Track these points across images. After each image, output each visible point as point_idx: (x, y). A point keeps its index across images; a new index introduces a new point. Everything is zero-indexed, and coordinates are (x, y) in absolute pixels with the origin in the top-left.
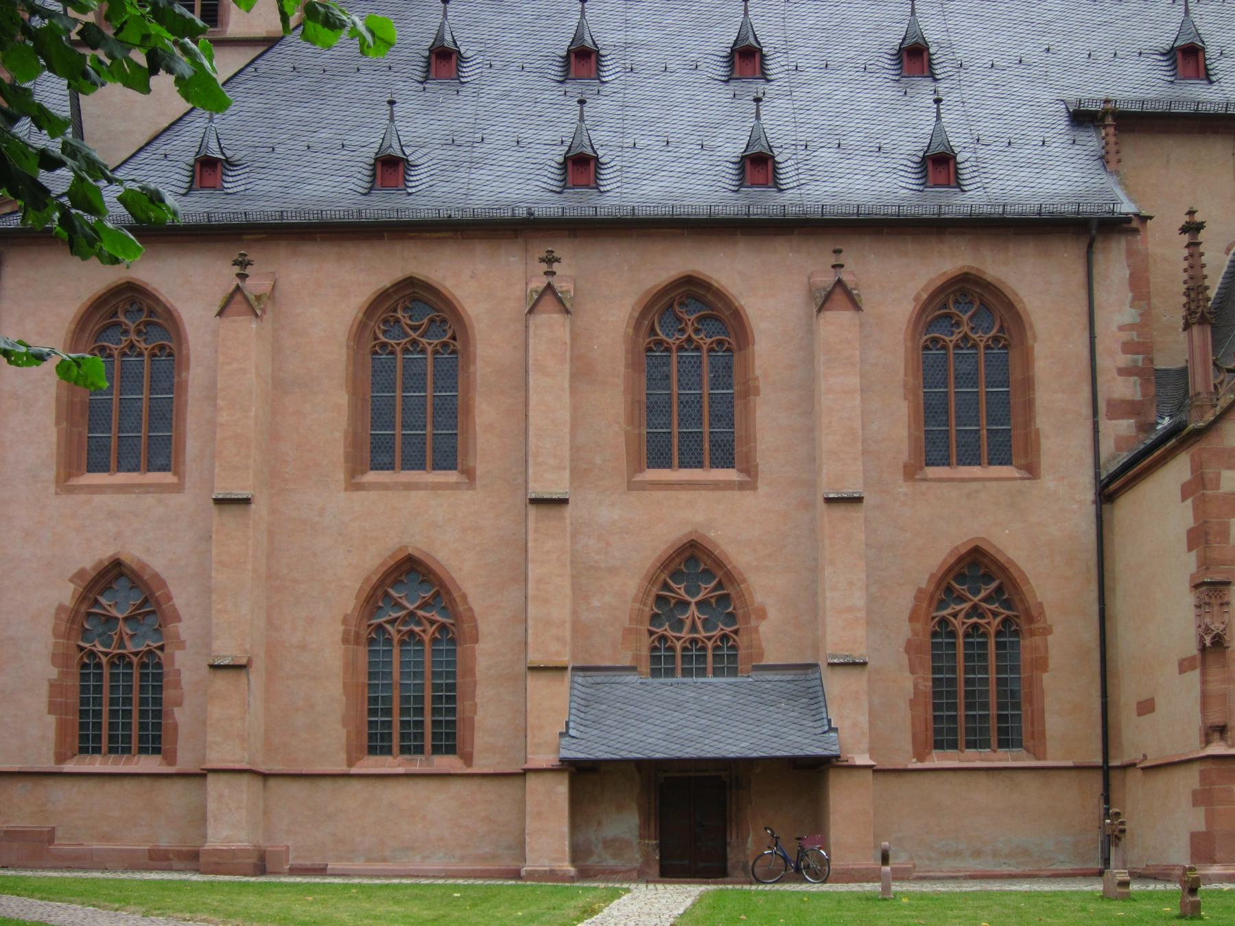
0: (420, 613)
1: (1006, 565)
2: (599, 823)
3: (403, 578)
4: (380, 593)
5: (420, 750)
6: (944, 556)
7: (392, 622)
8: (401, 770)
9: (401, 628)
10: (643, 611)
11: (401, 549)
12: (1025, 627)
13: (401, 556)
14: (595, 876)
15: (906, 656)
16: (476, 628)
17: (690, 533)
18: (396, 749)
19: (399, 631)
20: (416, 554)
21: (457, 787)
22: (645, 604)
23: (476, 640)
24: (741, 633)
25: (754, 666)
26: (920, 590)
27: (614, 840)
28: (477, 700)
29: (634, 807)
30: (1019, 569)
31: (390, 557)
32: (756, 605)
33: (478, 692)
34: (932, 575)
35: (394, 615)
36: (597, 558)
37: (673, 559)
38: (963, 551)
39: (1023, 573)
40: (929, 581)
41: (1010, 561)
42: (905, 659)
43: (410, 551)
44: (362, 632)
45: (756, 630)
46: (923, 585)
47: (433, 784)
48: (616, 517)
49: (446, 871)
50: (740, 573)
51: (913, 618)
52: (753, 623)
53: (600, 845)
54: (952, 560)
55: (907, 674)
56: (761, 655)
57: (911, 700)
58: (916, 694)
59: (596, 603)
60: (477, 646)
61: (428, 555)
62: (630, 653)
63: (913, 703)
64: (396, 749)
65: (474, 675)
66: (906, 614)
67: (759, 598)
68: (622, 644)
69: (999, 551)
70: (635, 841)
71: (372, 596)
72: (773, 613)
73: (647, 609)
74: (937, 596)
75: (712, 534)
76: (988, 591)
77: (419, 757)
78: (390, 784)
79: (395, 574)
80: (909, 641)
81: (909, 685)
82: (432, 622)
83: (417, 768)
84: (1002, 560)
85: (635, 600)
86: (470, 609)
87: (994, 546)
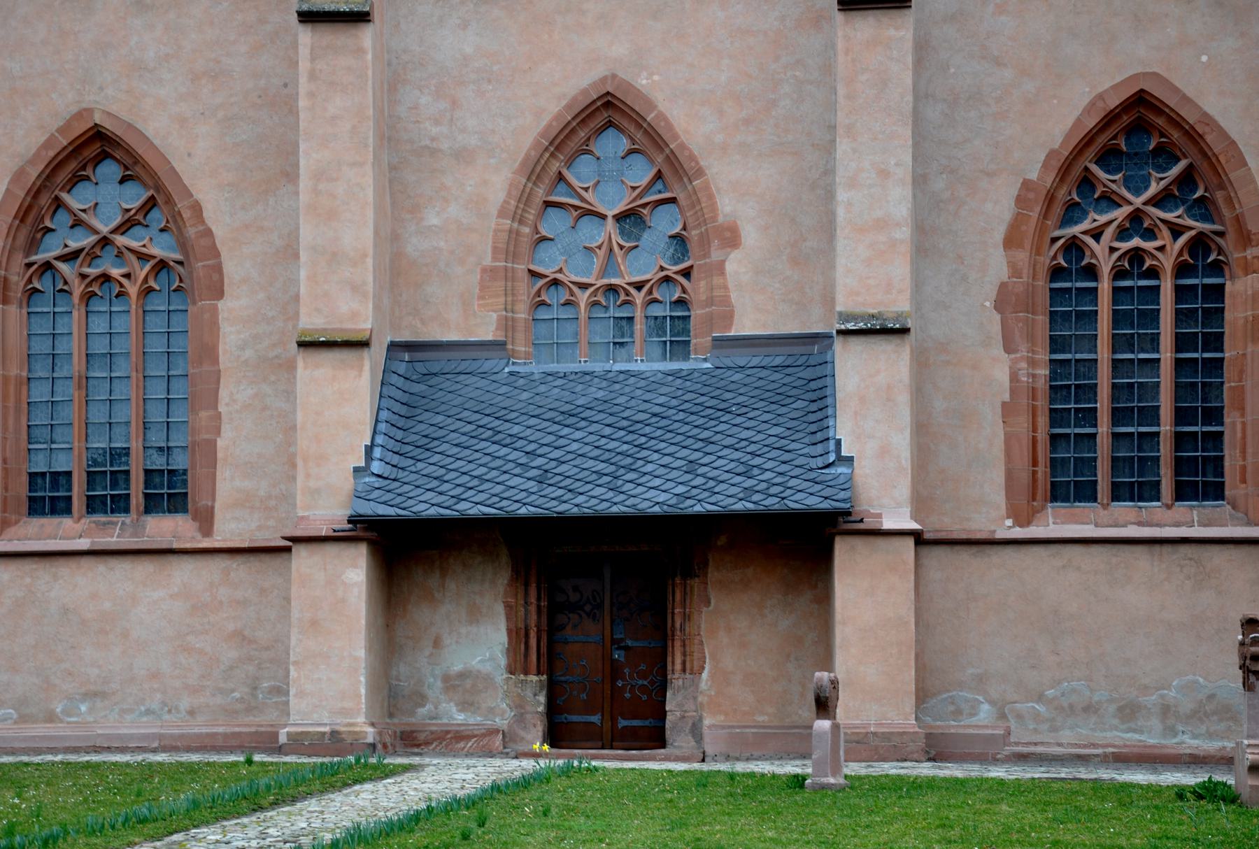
0: (121, 240)
1: (1199, 129)
2: (437, 643)
3: (89, 172)
4: (45, 200)
5: (120, 505)
6: (1077, 113)
7: (70, 257)
8: (83, 544)
9: (87, 270)
10: (518, 233)
11: (79, 115)
12: (1235, 255)
13: (80, 128)
14: (427, 743)
15: (998, 317)
16: (218, 269)
17: (604, 80)
18: (78, 503)
19: (83, 276)
20: (108, 125)
21: (183, 572)
22: (521, 222)
23: (220, 294)
24: (695, 274)
25: (715, 339)
26: (1026, 185)
27: (462, 675)
28: (222, 408)
29: (500, 609)
30: (1224, 134)
31: (61, 130)
32: (721, 219)
33: (223, 394)
34: (1051, 154)
35: (74, 245)
36: (435, 130)
37: (573, 131)
38: (1114, 102)
39: (1233, 143)
40: (1045, 165)
41: (1208, 120)
42: (994, 323)
43: (98, 118)
44: (14, 278)
45: (720, 268)
46: (1033, 176)
47: (145, 567)
48: (469, 50)
49: (161, 737)
50: (692, 158)
51: (1011, 241)
52: (716, 255)
53: (439, 684)
54: (1091, 123)
55: (998, 351)
56: (728, 317)
57: (1004, 404)
58: (1013, 391)
59: (433, 220)
60: (221, 304)
61: (130, 126)
62: (495, 316)
63: (1007, 410)
64: (78, 503)
65: (216, 361)
66: (999, 234)
67: (727, 206)
68: (481, 298)
69: (1186, 99)
70: (500, 676)
71: (30, 207)
72: (750, 235)
73: (526, 230)
74: (1062, 194)
75: (642, 82)
76: (1163, 183)
77: (120, 518)
78: (64, 569)
79: (73, 165)
80: (1003, 286)
81: (1001, 375)
82: (143, 257)
83: (112, 540)
84: (1190, 117)
85: (502, 213)
86: (209, 233)
87: (1176, 90)
